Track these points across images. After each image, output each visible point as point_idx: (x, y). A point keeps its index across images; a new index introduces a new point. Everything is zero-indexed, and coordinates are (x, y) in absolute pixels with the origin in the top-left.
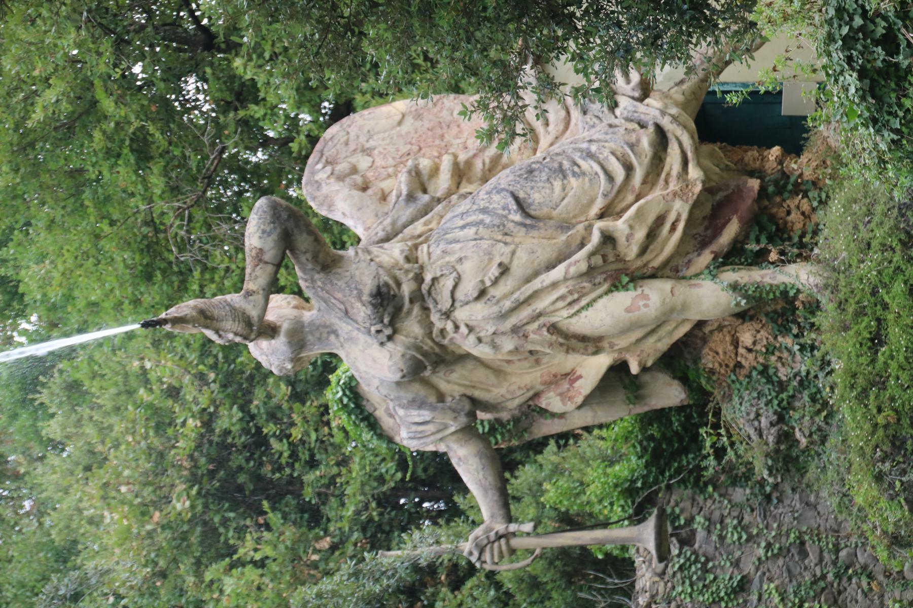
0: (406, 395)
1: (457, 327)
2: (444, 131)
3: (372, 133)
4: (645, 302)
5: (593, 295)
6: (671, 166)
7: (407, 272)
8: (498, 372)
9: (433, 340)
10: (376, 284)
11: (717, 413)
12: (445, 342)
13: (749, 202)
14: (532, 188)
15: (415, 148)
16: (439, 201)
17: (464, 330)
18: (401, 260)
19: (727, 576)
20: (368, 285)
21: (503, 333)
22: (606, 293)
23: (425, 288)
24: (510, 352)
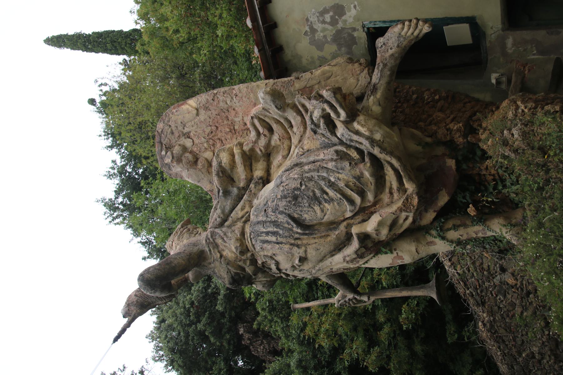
2: (227, 114)
3: (184, 123)
4: (401, 261)
6: (391, 182)
7: (245, 261)
10: (230, 276)
14: (301, 211)
15: (214, 128)
22: (374, 256)
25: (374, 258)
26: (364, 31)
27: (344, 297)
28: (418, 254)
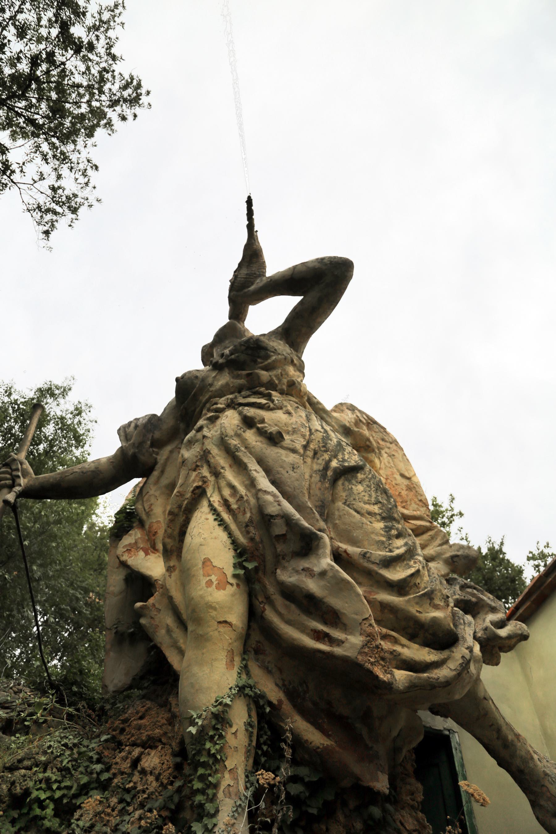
4: (215, 583)
5: (233, 527)
10: (269, 348)
22: (234, 543)
25: (229, 541)
26: (445, 729)
27: (25, 474)
28: (220, 622)
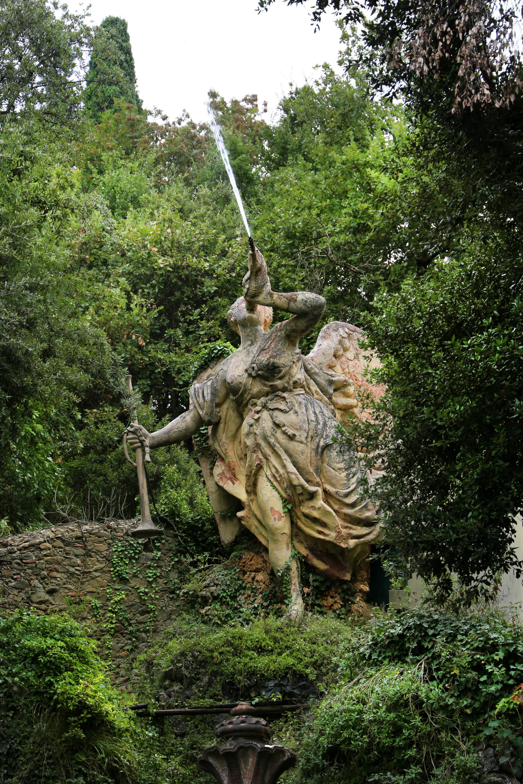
0: (219, 386)
1: (258, 412)
5: (280, 489)
7: (288, 383)
8: (235, 436)
9: (250, 399)
11: (217, 562)
12: (249, 406)
13: (337, 574)
16: (330, 398)
17: (257, 416)
18: (295, 379)
19: (127, 570)
20: (280, 361)
21: (255, 439)
23: (280, 393)
24: (245, 443)
